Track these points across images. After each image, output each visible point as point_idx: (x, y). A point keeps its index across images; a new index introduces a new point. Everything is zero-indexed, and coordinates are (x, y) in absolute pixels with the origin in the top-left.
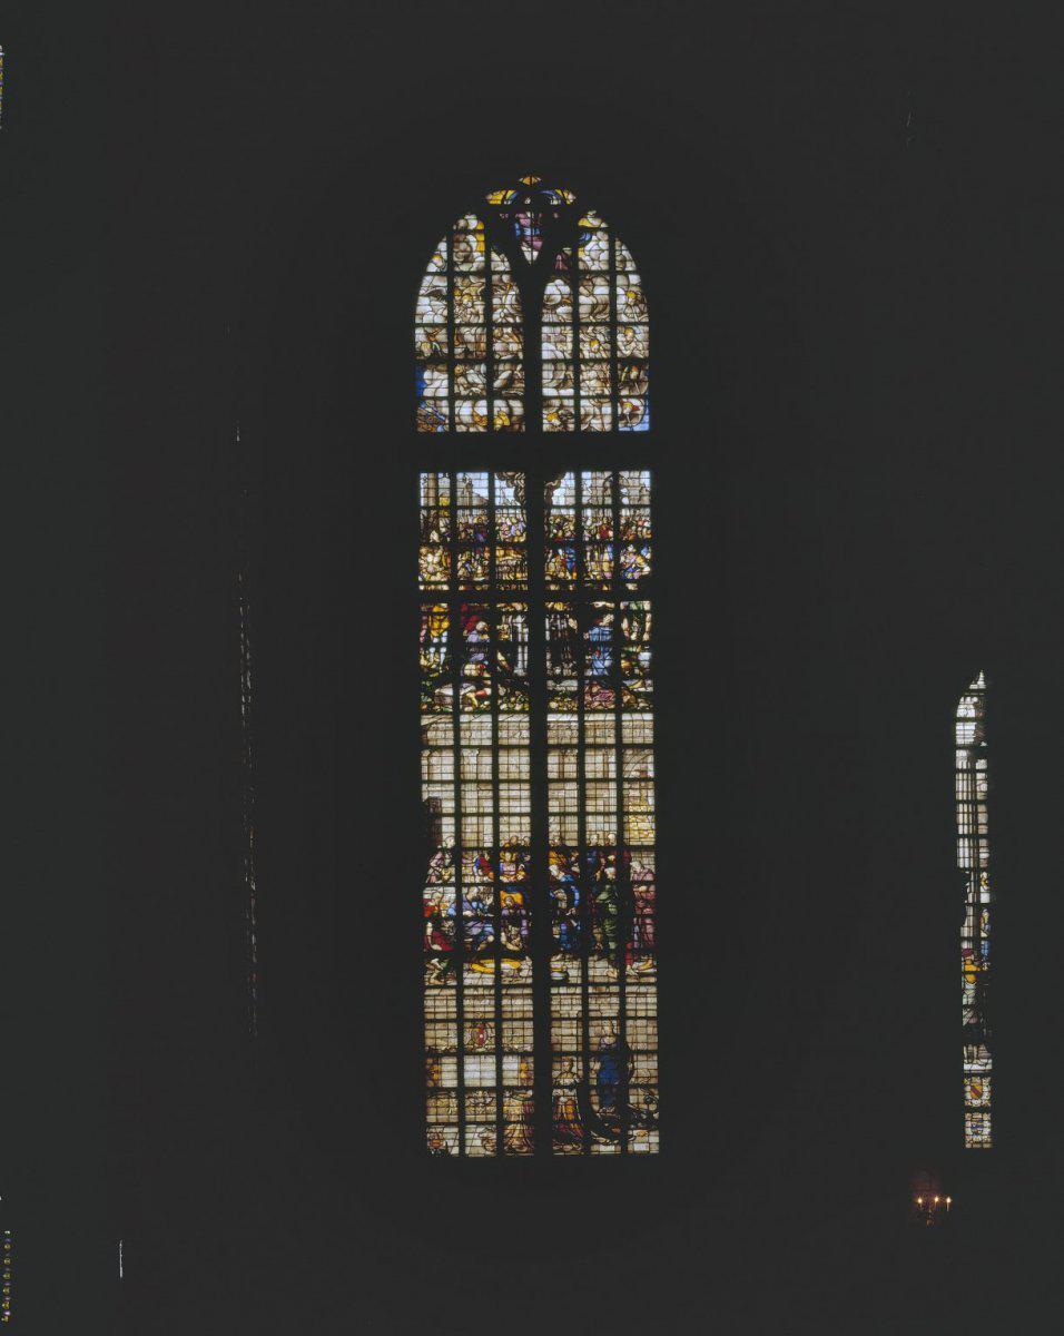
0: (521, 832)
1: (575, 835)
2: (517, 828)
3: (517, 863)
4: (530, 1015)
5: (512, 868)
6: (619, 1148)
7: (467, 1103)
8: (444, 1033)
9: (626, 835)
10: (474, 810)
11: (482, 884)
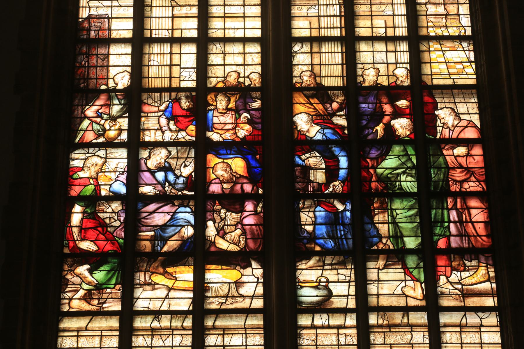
0: (244, 65)
1: (338, 70)
2: (239, 60)
3: (237, 111)
5: (229, 119)
9: (426, 69)
10: (166, 34)
11: (175, 143)
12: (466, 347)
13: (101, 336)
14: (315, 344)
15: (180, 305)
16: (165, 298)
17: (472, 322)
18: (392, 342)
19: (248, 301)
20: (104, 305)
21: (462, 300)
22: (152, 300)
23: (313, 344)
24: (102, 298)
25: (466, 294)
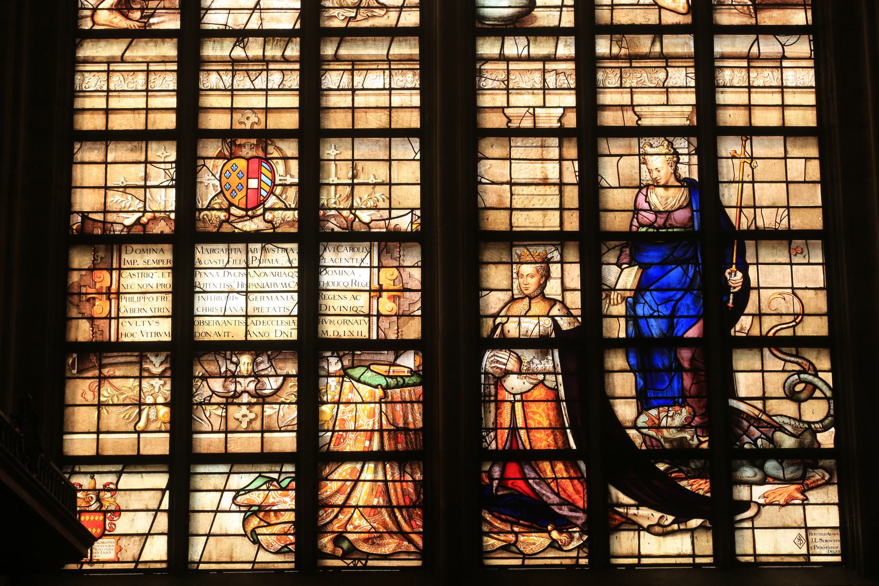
4: (413, 120)
6: (705, 544)
7: (203, 392)
8: (135, 174)
12: (756, 92)
13: (148, 72)
14: (504, 87)
15: (279, 21)
16: (254, 9)
17: (768, 51)
18: (634, 85)
19: (393, 15)
20: (152, 21)
21: (753, 15)
22: (231, 11)
23: (501, 87)
24: (147, 9)
25: (760, 4)
